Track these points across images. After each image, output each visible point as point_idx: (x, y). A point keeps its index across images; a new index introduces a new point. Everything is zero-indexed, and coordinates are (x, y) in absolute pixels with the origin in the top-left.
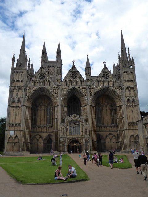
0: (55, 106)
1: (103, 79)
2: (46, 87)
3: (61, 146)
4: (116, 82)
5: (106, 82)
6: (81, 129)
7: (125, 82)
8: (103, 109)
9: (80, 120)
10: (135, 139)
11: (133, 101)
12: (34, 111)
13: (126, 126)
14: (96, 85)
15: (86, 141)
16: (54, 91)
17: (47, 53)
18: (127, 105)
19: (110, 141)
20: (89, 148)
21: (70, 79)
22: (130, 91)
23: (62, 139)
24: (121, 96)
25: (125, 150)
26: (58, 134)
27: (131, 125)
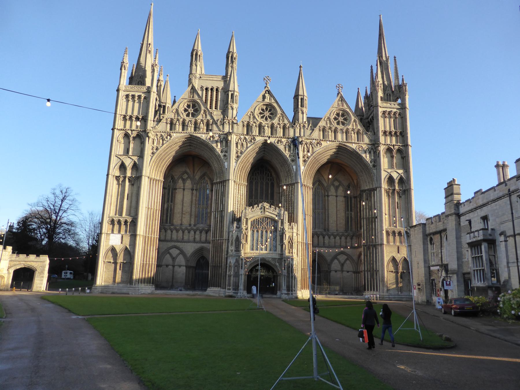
0: (219, 183)
2: (199, 135)
3: (230, 276)
6: (278, 238)
8: (328, 196)
11: (401, 181)
12: (167, 191)
14: (317, 138)
19: (339, 267)
23: (232, 261)
25: (374, 290)
26: (224, 247)
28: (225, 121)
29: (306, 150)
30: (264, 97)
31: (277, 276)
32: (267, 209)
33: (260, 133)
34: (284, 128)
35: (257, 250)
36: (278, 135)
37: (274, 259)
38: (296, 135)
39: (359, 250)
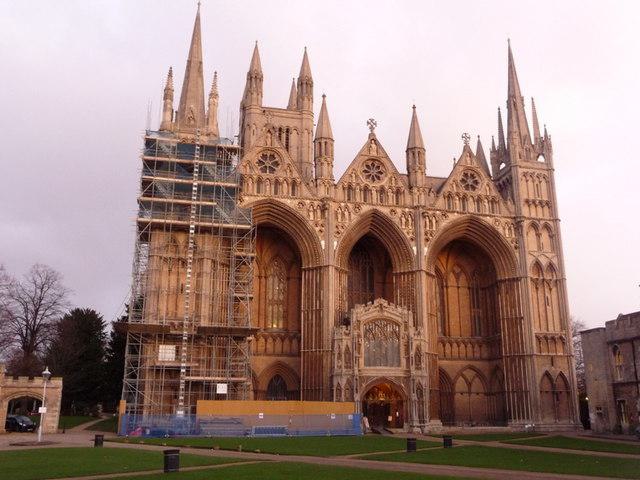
1: (462, 190)
2: (282, 200)
4: (501, 204)
5: (471, 199)
6: (402, 349)
7: (526, 205)
8: (447, 287)
9: (400, 320)
10: (553, 386)
13: (531, 346)
15: (420, 390)
16: (312, 218)
17: (261, 80)
20: (426, 410)
21: (365, 181)
22: (538, 235)
24: (516, 248)
26: (326, 362)
27: (543, 341)
28: (319, 181)
31: (402, 402)
34: (398, 192)
35: (375, 364)
36: (390, 202)
37: (398, 378)
39: (495, 363)
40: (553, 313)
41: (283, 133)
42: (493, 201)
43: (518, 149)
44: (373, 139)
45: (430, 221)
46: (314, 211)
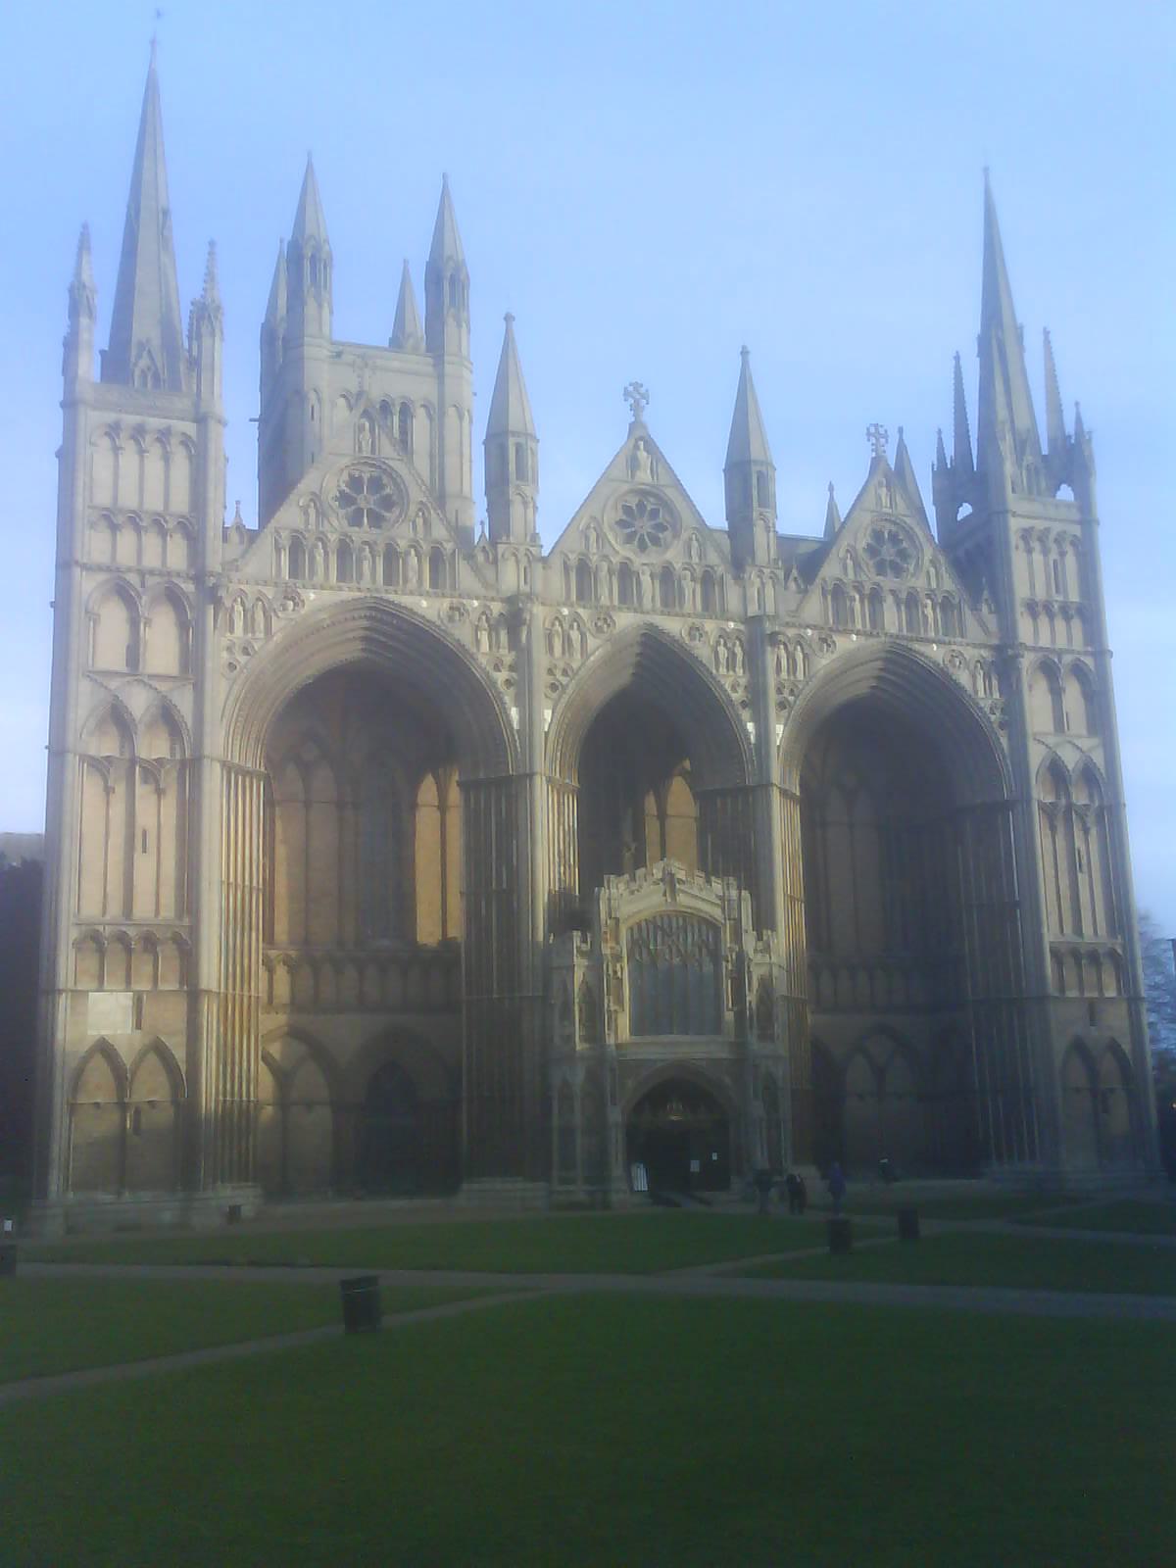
2: (406, 600)
9: (717, 913)
16: (485, 646)
17: (328, 264)
18: (1039, 802)
22: (1056, 693)
27: (1069, 961)
28: (501, 548)
29: (784, 662)
30: (633, 464)
32: (680, 881)
33: (624, 597)
34: (708, 580)
36: (688, 607)
38: (753, 610)
40: (1092, 890)
41: (385, 414)
42: (946, 605)
43: (1009, 468)
44: (640, 440)
45: (791, 657)
46: (493, 629)
